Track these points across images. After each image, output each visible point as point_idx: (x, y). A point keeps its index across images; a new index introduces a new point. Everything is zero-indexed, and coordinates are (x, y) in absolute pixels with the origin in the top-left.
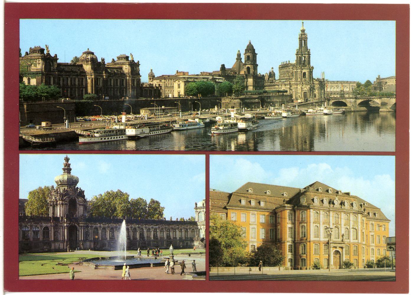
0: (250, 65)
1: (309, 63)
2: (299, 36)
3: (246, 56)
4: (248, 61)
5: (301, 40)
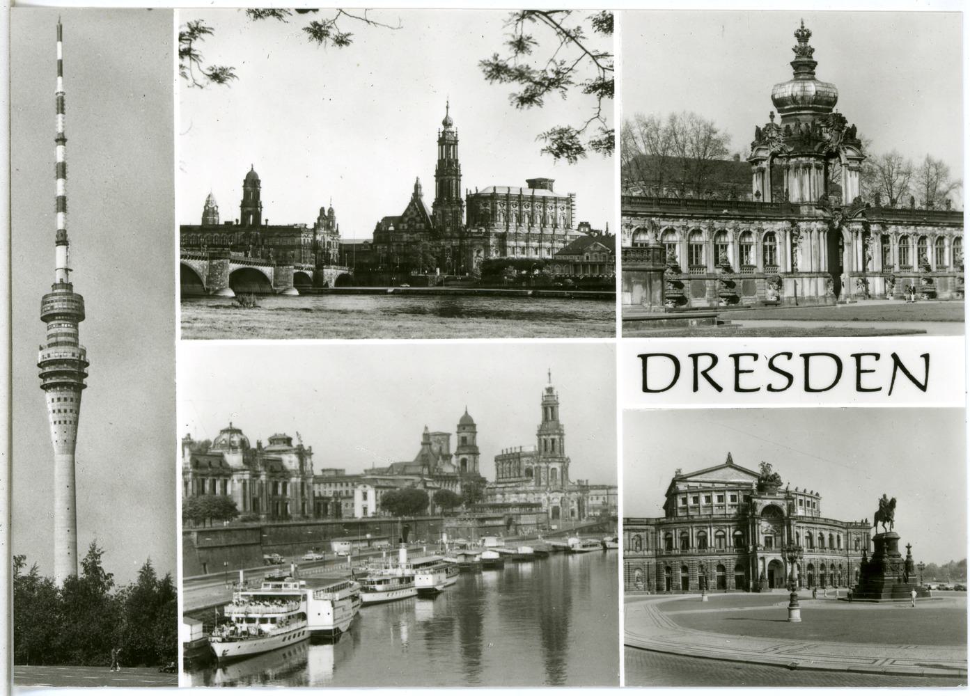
0: (467, 454)
1: (562, 450)
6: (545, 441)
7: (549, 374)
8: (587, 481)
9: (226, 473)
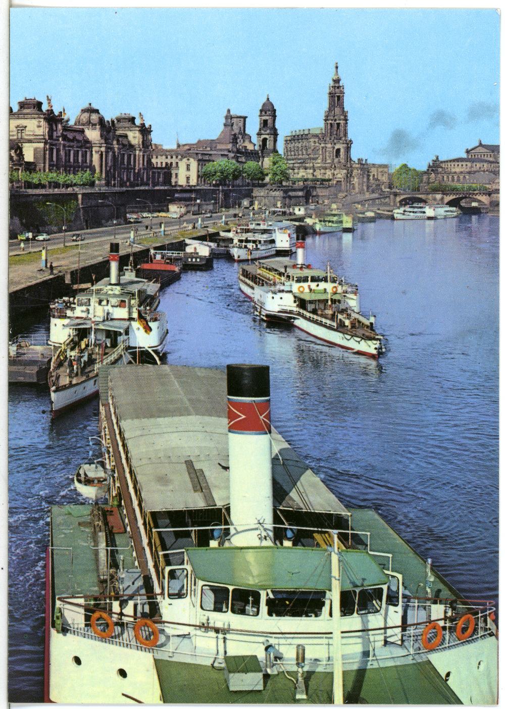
0: (268, 134)
1: (346, 134)
3: (262, 122)
4: (264, 129)
5: (332, 95)
7: (337, 67)
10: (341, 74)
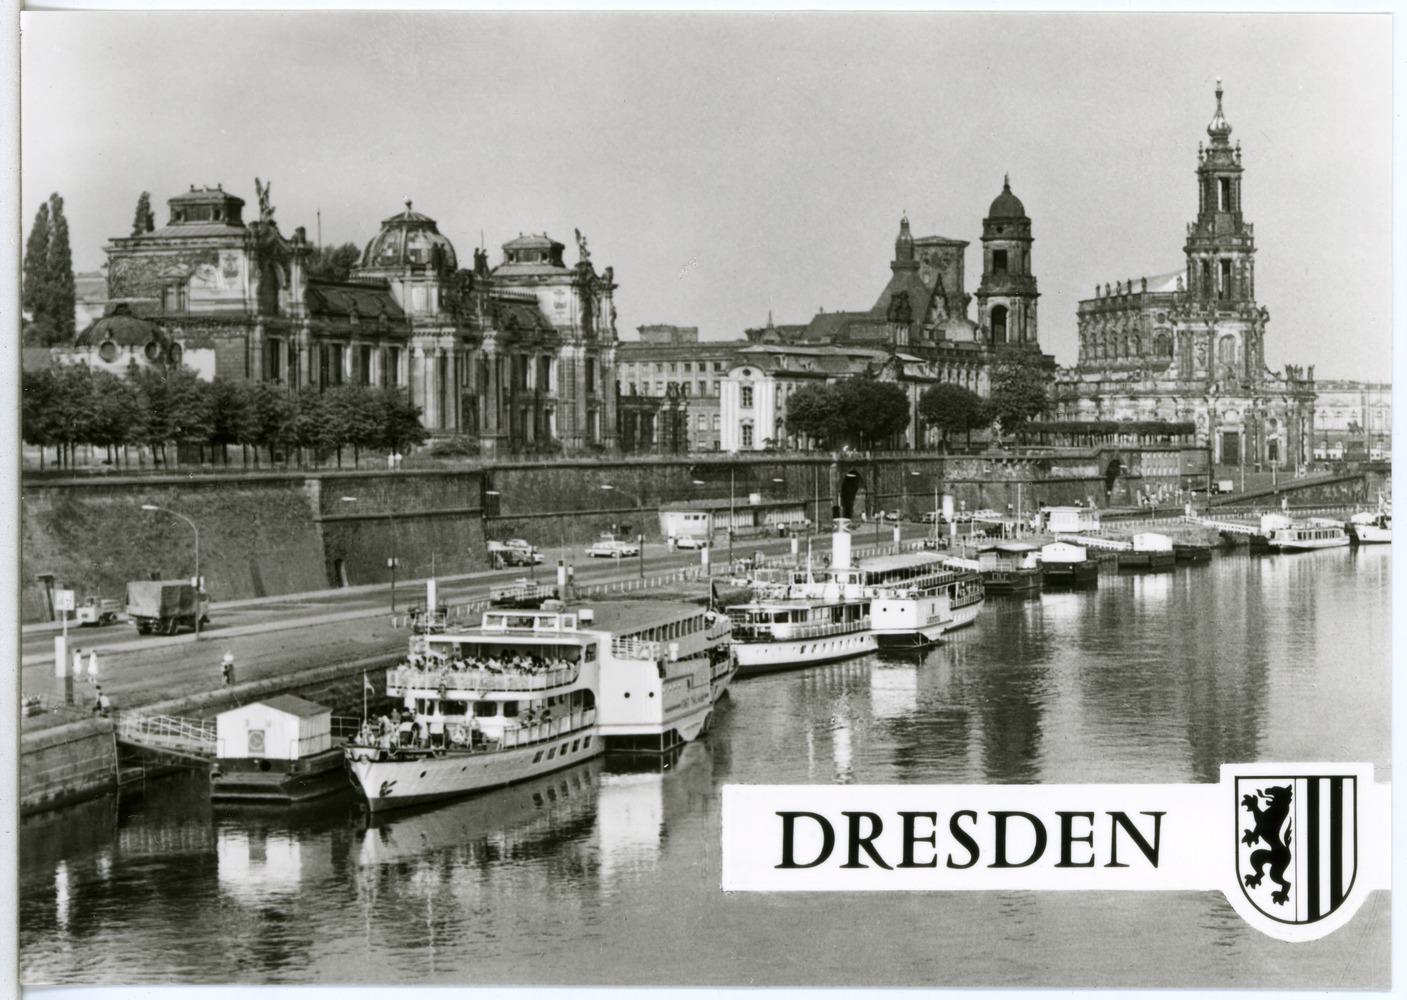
0: (1007, 295)
1: (1247, 293)
2: (1201, 158)
3: (990, 255)
5: (1205, 175)
6: (1206, 264)
7: (1219, 94)
8: (1310, 369)
9: (394, 330)
10: (1229, 119)
